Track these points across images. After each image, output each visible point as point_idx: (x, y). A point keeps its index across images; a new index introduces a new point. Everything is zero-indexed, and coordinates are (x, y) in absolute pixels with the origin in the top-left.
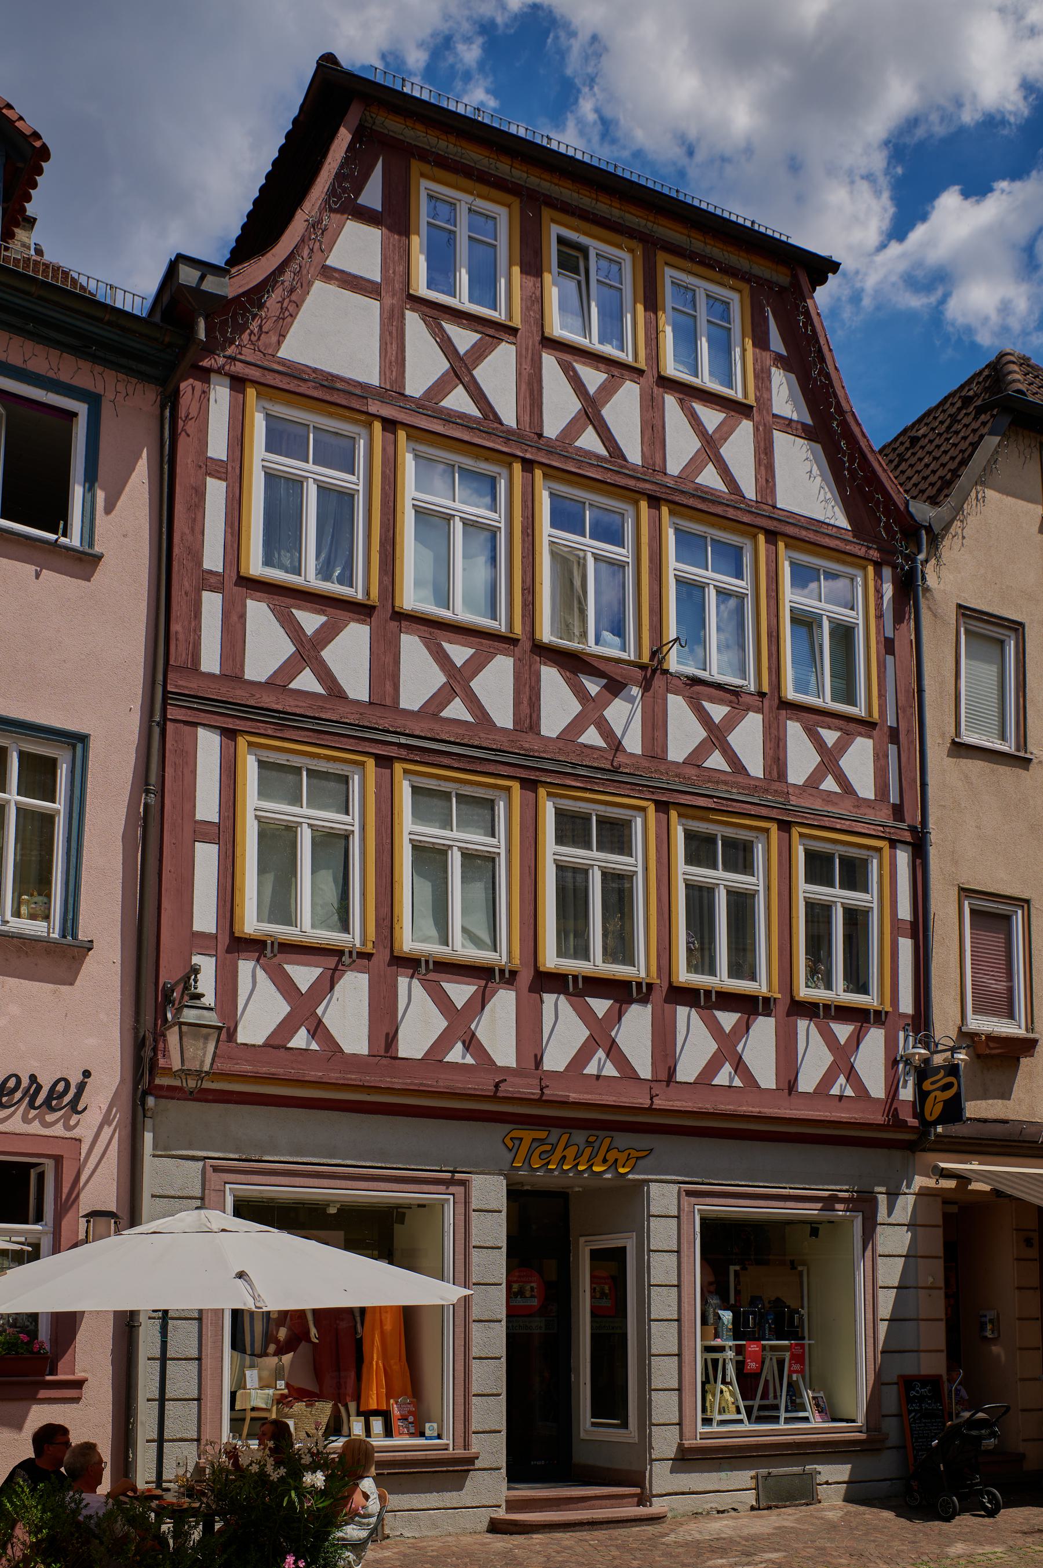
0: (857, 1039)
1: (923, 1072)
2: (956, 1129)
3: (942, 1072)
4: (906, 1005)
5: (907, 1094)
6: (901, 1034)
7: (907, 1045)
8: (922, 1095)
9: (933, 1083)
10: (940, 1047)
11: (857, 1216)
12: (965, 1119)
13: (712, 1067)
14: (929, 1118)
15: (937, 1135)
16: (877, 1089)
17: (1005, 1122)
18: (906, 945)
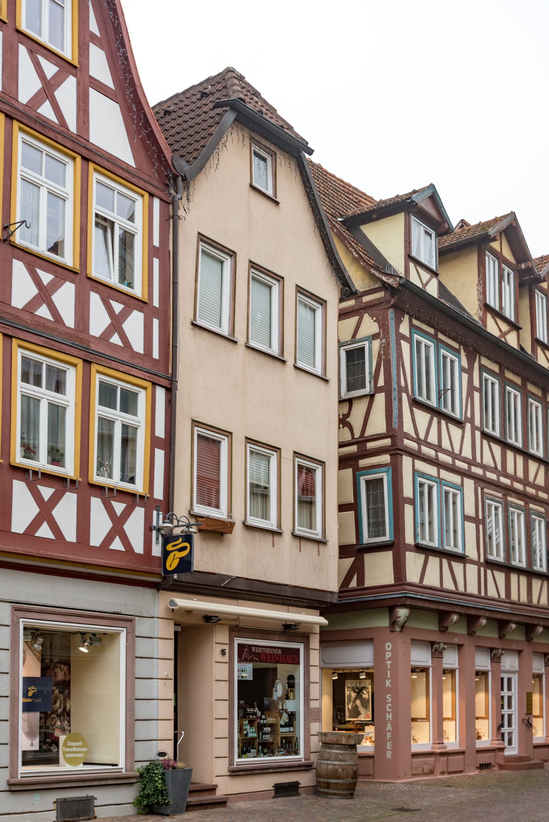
0: (127, 513)
1: (168, 539)
2: (185, 577)
3: (181, 539)
4: (159, 494)
5: (157, 551)
6: (155, 513)
7: (157, 519)
8: (166, 553)
9: (173, 546)
10: (181, 523)
11: (123, 631)
12: (192, 570)
13: (35, 524)
14: (169, 569)
15: (175, 580)
16: (139, 548)
17: (214, 574)
18: (160, 454)
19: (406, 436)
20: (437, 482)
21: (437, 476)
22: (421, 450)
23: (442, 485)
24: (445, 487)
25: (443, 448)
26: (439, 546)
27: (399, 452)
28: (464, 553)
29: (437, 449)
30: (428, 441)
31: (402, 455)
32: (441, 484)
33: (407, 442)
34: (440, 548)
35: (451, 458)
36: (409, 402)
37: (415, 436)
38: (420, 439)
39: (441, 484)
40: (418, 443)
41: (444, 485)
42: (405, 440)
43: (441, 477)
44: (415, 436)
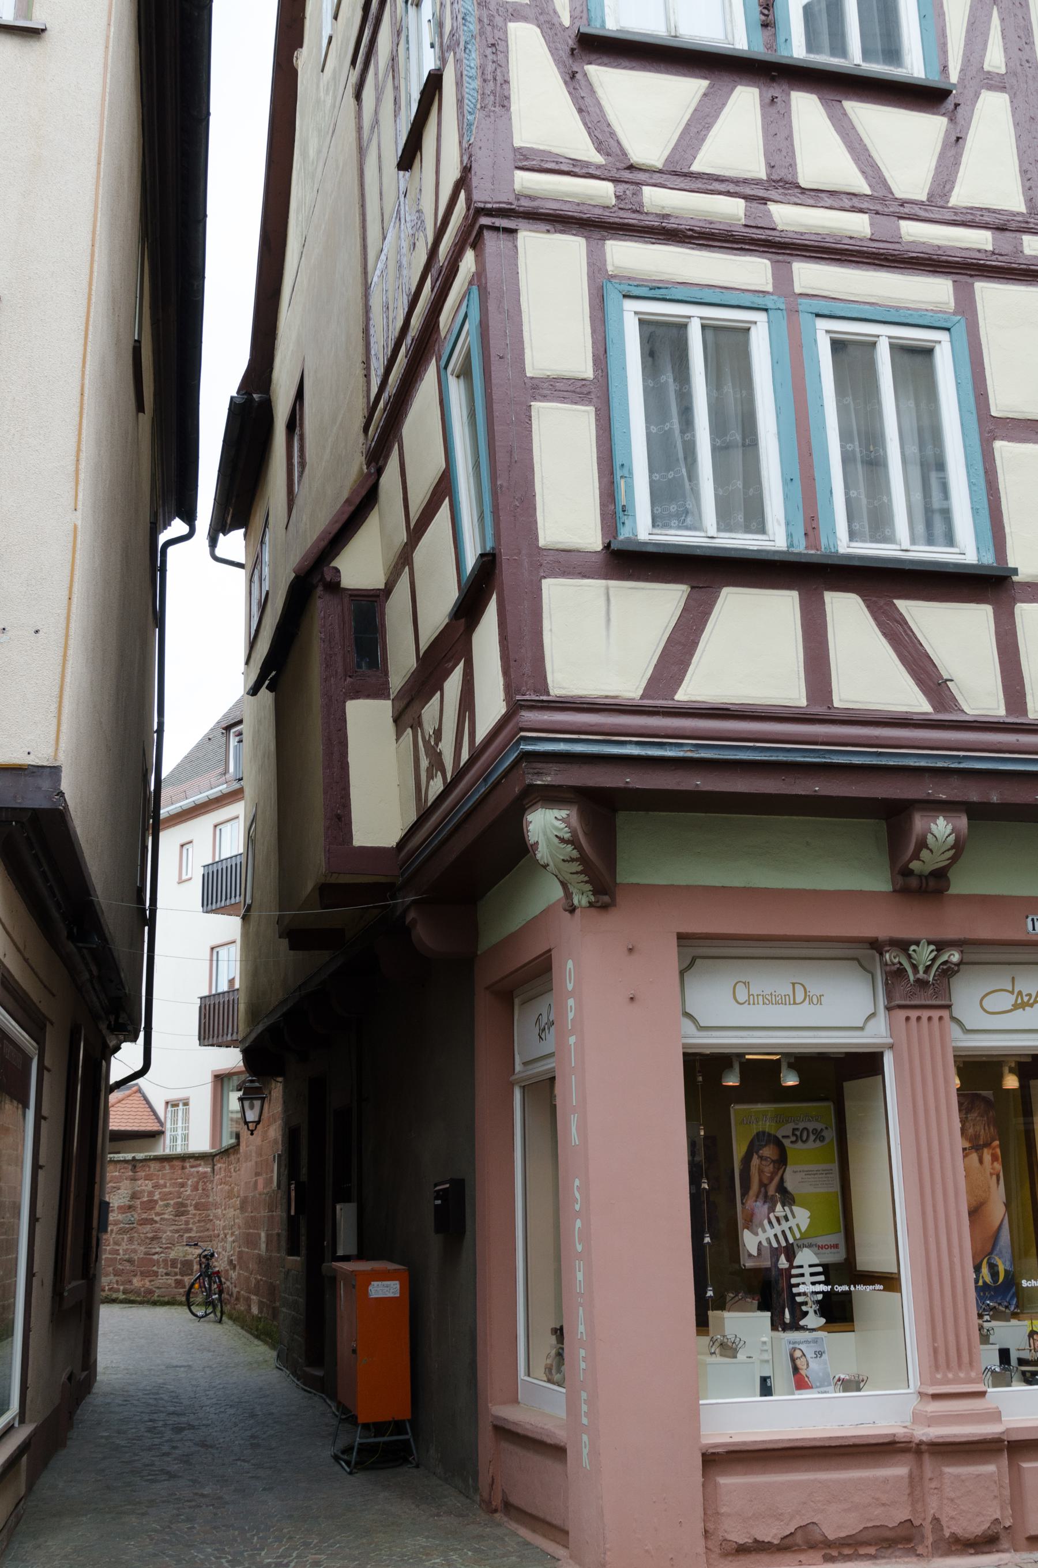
19: (527, 159)
20: (766, 310)
21: (769, 288)
22: (641, 205)
23: (805, 318)
24: (823, 324)
25: (802, 186)
26: (791, 545)
27: (484, 221)
28: (989, 559)
29: (761, 193)
30: (696, 167)
31: (512, 232)
32: (793, 312)
33: (526, 181)
34: (800, 547)
35: (865, 218)
36: (553, 51)
37: (598, 159)
38: (631, 168)
39: (793, 312)
40: (615, 181)
41: (818, 315)
42: (519, 174)
43: (798, 290)
44: (598, 159)
